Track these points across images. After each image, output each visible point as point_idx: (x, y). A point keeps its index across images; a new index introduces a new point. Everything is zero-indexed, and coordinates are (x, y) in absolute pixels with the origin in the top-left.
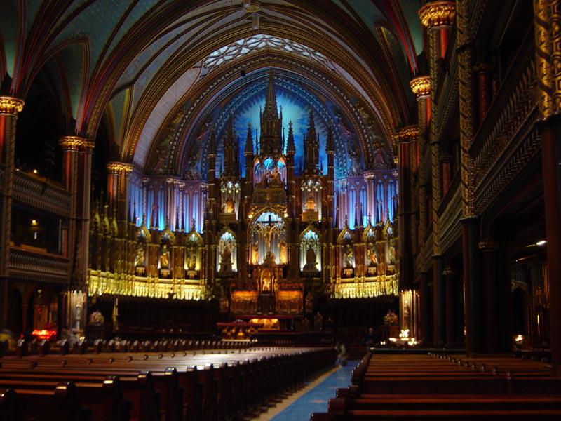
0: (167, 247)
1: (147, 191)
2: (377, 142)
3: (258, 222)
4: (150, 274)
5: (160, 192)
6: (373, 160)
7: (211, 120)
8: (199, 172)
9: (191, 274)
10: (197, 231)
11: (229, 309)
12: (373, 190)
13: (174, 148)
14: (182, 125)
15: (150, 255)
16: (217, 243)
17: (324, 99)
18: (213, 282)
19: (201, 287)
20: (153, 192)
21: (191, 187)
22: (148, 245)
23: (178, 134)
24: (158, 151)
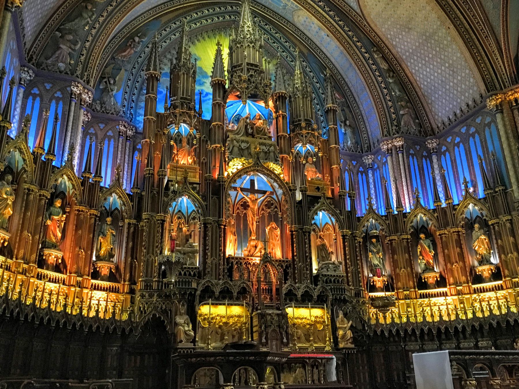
0: (63, 207)
1: (26, 97)
2: (402, 101)
3: (235, 189)
4: (22, 252)
5: (54, 103)
6: (399, 123)
7: (144, 35)
8: (119, 105)
9: (105, 268)
10: (124, 187)
11: (194, 341)
12: (401, 163)
13: (90, 38)
14: (110, 8)
15: (26, 209)
16: (166, 212)
17: (305, 51)
18: (155, 286)
19: (121, 297)
20: (38, 99)
21: (102, 126)
22: (26, 186)
23: (101, 19)
24: (58, 34)
